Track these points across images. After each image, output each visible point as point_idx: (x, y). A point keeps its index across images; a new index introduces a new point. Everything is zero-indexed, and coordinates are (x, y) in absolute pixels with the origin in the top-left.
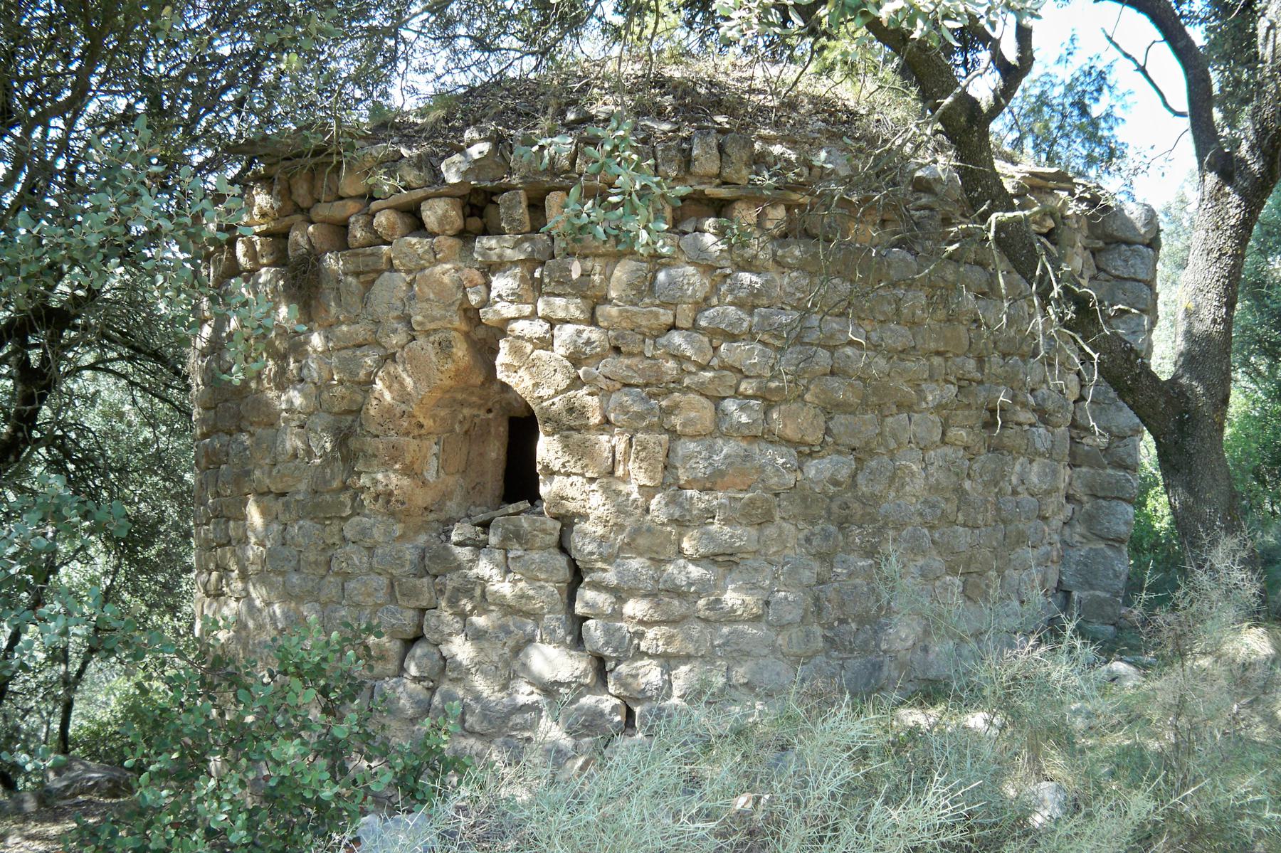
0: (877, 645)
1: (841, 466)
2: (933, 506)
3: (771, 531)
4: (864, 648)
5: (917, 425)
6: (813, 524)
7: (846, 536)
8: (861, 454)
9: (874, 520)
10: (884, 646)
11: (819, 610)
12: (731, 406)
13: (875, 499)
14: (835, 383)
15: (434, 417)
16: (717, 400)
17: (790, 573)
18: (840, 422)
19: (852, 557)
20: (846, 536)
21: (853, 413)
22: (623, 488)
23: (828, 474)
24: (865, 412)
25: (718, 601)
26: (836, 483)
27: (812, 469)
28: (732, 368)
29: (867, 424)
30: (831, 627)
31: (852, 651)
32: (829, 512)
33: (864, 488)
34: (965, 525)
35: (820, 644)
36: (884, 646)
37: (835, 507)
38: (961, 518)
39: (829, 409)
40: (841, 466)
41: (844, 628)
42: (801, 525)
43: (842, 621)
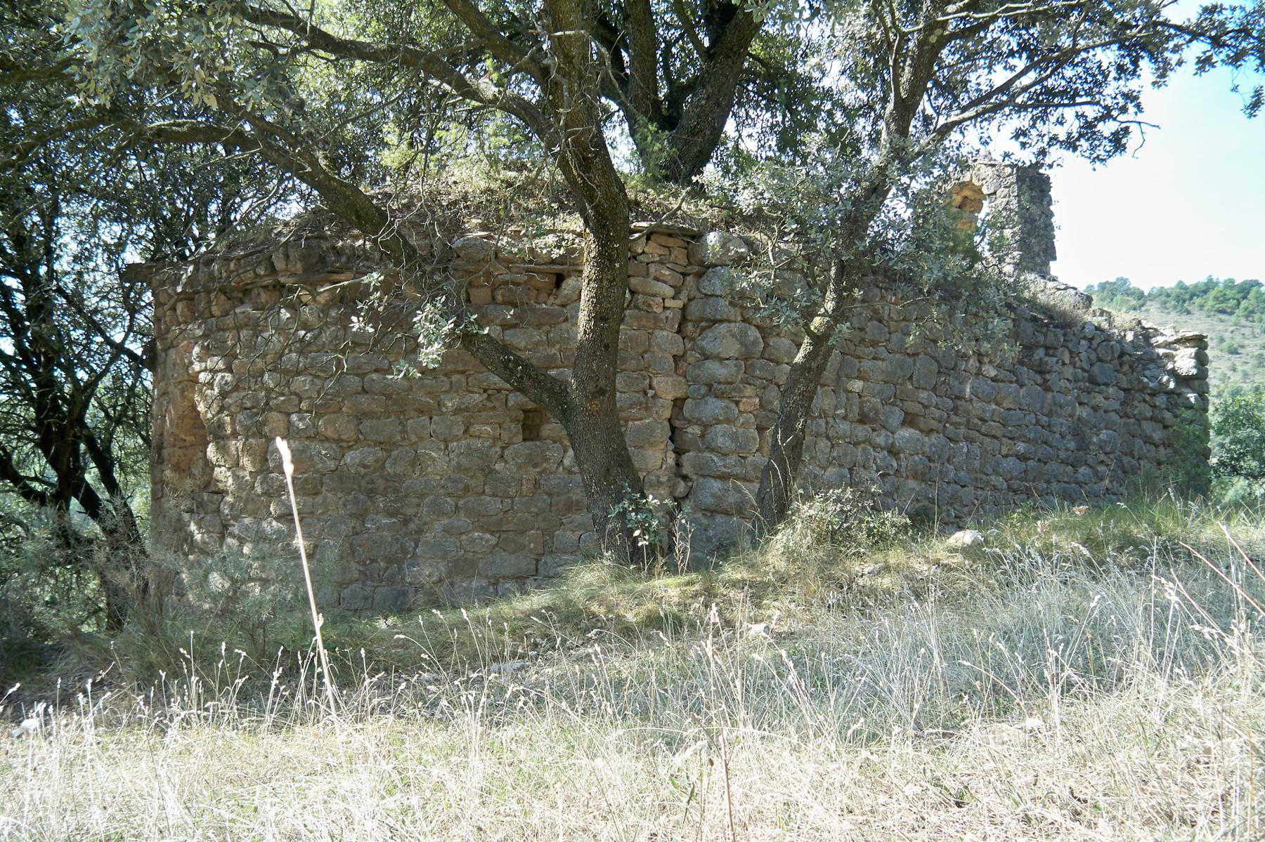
0: (403, 579)
1: (370, 455)
2: (454, 481)
3: (319, 499)
4: (392, 581)
5: (436, 424)
6: (349, 494)
7: (374, 503)
8: (387, 446)
9: (396, 491)
10: (408, 580)
11: (353, 552)
12: (294, 417)
13: (400, 478)
14: (362, 399)
15: (194, 435)
16: (288, 414)
17: (331, 527)
18: (367, 424)
19: (379, 517)
20: (374, 503)
21: (378, 418)
22: (241, 473)
23: (357, 461)
24: (389, 417)
25: (288, 545)
26: (365, 467)
27: (351, 457)
28: (295, 394)
29: (389, 426)
30: (365, 564)
31: (381, 581)
32: (360, 486)
33: (389, 469)
34: (494, 495)
35: (356, 575)
36: (408, 580)
37: (363, 483)
38: (487, 490)
39: (360, 417)
40: (370, 455)
41: (375, 565)
42: (340, 495)
43: (373, 561)
